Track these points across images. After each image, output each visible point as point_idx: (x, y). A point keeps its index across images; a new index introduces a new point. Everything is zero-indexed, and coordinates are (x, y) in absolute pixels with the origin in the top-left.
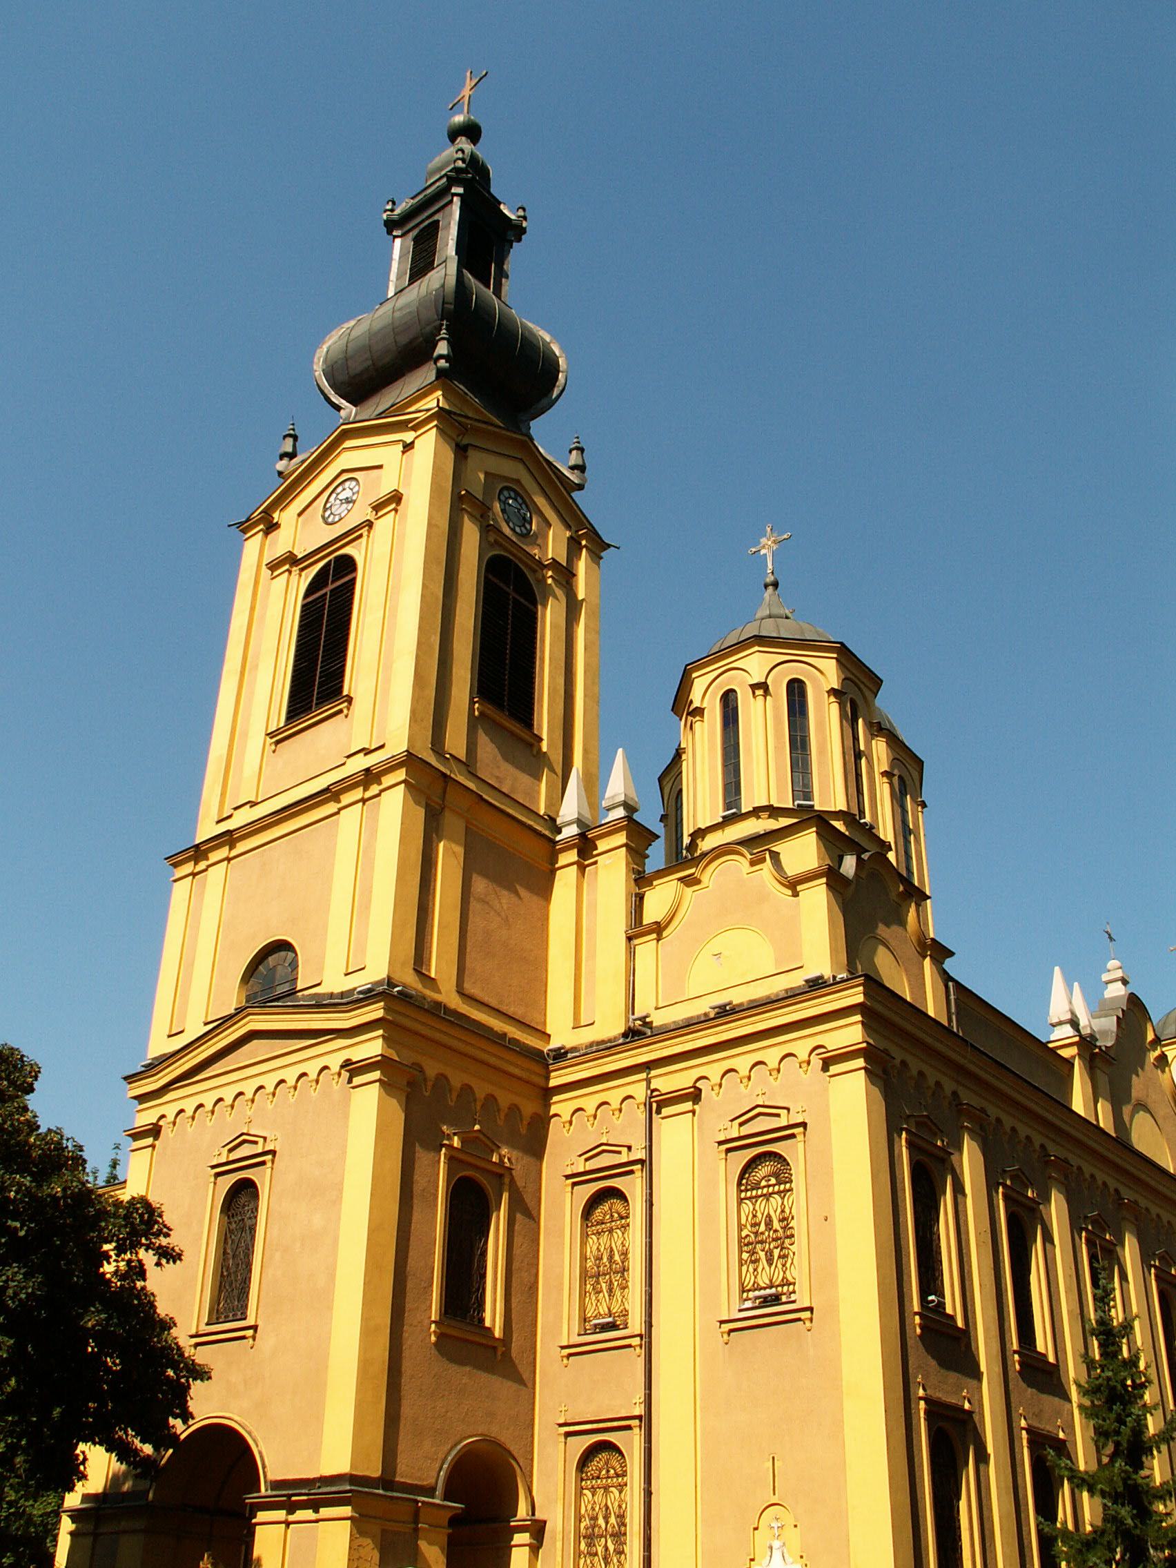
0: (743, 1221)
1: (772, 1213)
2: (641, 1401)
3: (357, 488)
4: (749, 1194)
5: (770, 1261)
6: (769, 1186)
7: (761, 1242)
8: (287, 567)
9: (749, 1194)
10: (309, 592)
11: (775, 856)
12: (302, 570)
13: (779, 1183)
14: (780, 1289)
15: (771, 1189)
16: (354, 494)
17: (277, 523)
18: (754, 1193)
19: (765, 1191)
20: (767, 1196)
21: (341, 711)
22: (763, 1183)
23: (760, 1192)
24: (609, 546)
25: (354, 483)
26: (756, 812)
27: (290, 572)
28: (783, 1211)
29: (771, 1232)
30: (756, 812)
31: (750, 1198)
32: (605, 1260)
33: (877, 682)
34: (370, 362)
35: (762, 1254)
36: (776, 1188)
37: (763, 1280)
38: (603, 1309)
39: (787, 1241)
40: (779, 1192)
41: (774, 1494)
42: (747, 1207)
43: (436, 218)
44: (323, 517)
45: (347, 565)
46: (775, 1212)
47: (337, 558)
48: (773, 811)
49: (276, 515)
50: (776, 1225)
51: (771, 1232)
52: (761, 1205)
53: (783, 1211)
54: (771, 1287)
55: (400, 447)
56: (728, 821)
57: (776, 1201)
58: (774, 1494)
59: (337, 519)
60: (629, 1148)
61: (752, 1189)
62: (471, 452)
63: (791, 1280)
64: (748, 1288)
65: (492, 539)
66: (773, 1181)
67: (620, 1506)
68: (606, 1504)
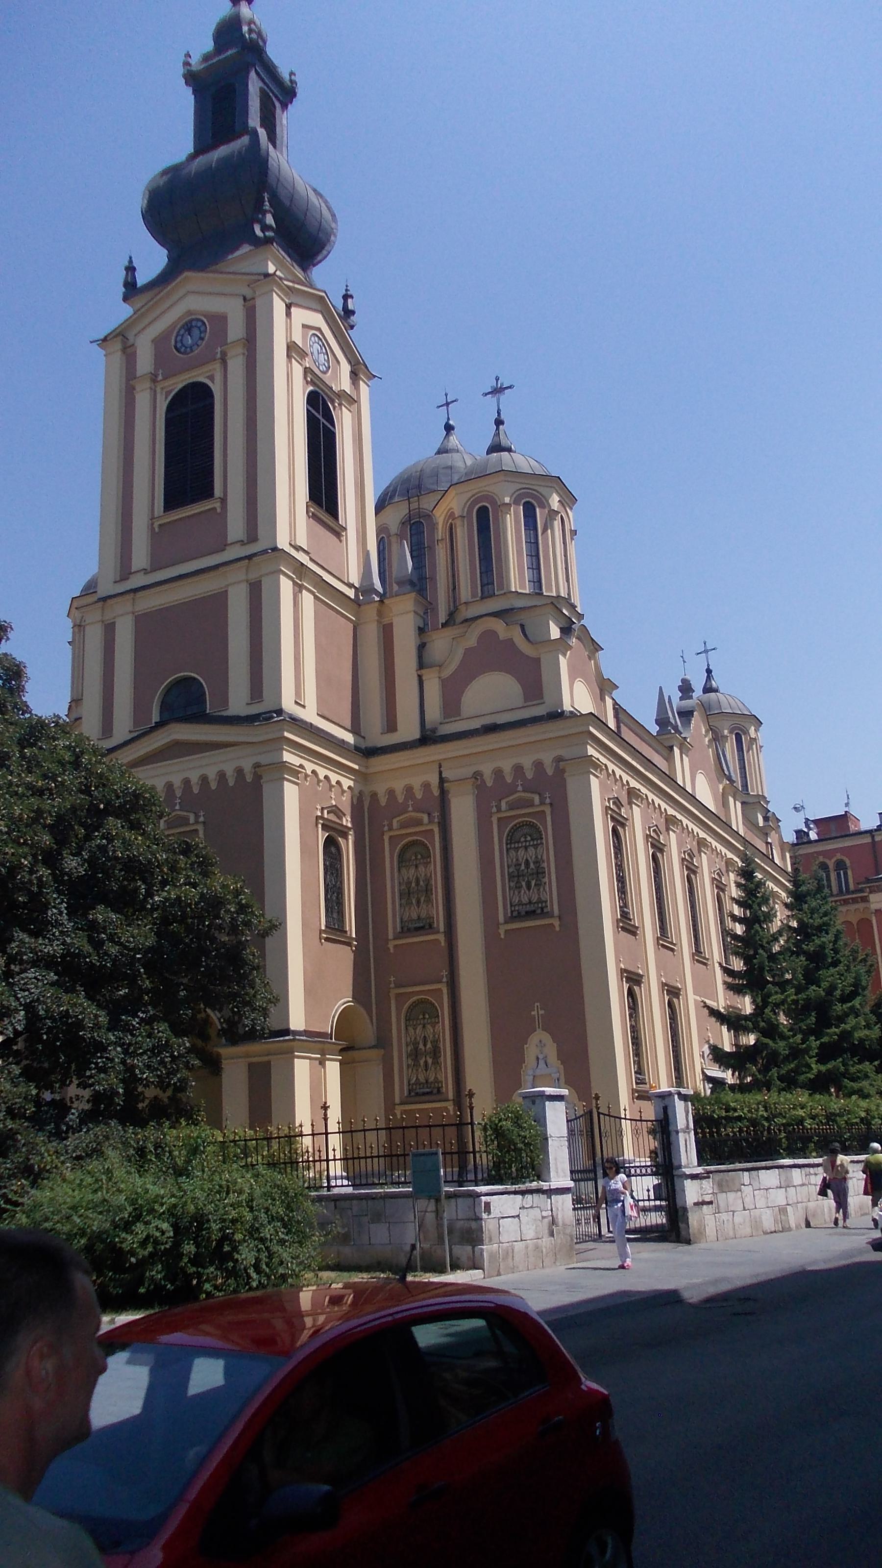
1: (529, 859)
5: (529, 887)
6: (526, 841)
7: (523, 876)
10: (170, 409)
13: (532, 840)
16: (201, 333)
17: (133, 345)
20: (526, 848)
21: (214, 509)
24: (375, 376)
28: (536, 857)
36: (532, 843)
37: (525, 900)
40: (533, 845)
42: (513, 853)
44: (176, 347)
46: (531, 858)
49: (131, 336)
50: (532, 866)
53: (536, 857)
57: (531, 850)
60: (429, 814)
61: (515, 843)
63: (543, 899)
66: (529, 838)
67: (434, 1036)
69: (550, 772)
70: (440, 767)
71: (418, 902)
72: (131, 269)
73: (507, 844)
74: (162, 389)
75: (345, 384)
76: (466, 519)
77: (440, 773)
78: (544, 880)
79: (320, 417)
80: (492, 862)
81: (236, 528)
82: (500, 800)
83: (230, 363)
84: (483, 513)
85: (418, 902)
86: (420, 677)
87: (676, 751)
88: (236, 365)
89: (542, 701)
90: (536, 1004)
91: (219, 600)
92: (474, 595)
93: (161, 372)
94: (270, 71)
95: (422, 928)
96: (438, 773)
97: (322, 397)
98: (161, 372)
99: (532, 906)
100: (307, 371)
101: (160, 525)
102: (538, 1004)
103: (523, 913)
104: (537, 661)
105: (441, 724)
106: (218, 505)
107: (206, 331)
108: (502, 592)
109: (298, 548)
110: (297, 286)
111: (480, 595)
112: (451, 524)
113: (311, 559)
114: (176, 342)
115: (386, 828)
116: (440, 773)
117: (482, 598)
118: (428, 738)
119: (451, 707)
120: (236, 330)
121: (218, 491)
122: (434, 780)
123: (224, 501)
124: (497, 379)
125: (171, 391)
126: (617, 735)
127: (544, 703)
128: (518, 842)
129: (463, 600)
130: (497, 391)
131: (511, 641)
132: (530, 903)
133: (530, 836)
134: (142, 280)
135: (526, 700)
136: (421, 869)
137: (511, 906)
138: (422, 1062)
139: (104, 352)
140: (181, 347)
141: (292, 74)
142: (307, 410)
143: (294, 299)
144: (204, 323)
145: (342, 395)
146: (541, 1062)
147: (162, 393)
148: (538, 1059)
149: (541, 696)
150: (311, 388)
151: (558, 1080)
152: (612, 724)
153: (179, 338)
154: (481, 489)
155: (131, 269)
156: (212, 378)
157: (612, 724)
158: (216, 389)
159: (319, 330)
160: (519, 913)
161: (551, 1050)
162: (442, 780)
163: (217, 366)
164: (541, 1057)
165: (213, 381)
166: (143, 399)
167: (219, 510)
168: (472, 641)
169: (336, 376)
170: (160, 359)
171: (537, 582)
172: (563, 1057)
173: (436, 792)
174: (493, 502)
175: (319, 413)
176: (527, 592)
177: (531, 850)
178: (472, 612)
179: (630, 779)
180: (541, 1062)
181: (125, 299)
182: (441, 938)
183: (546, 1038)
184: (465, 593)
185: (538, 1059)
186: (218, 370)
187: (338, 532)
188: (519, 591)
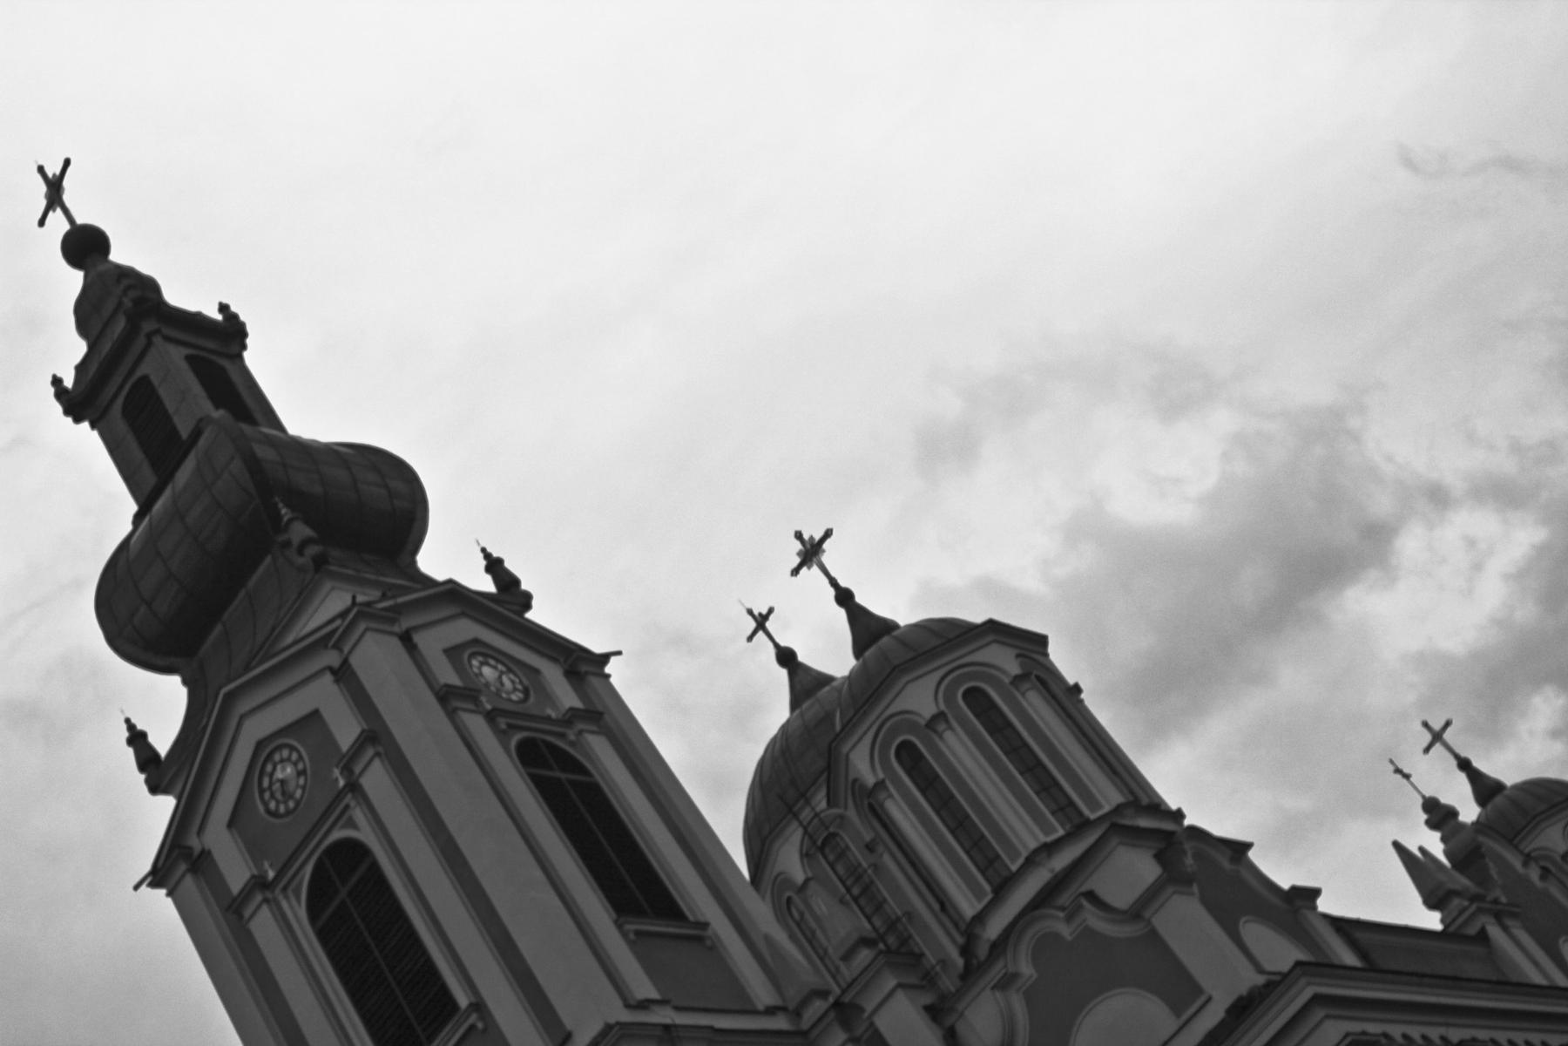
3: (294, 756)
8: (259, 897)
10: (314, 912)
11: (1091, 896)
12: (285, 889)
16: (295, 764)
21: (472, 1027)
25: (285, 753)
26: (1031, 861)
27: (266, 900)
30: (1031, 861)
33: (1041, 641)
43: (139, 373)
44: (268, 812)
45: (353, 852)
48: (1049, 849)
49: (194, 842)
55: (328, 678)
56: (1003, 886)
62: (418, 638)
65: (503, 726)
72: (137, 738)
75: (568, 698)
76: (888, 783)
79: (563, 776)
83: (367, 782)
84: (909, 756)
87: (1494, 931)
88: (377, 779)
89: (1203, 999)
92: (978, 893)
93: (266, 865)
94: (192, 322)
97: (544, 741)
98: (266, 865)
100: (491, 717)
106: (473, 1018)
107: (301, 757)
108: (1020, 861)
109: (644, 1005)
110: (400, 600)
111: (987, 888)
113: (678, 1009)
114: (266, 804)
120: (346, 730)
123: (478, 1006)
124: (799, 536)
125: (300, 884)
126: (1372, 969)
127: (1209, 999)
130: (811, 552)
131: (1088, 933)
134: (162, 742)
135: (1178, 1014)
139: (163, 892)
140: (277, 806)
141: (223, 308)
142: (530, 775)
143: (406, 623)
144: (292, 748)
145: (572, 716)
147: (287, 898)
149: (1197, 990)
150: (516, 738)
152: (1349, 958)
153: (267, 795)
154: (880, 720)
155: (137, 738)
156: (352, 824)
157: (1349, 958)
158: (365, 834)
159: (476, 641)
163: (348, 798)
166: (263, 925)
167: (480, 1025)
169: (547, 697)
170: (255, 849)
171: (1064, 808)
174: (912, 727)
175: (551, 768)
176: (1061, 832)
178: (994, 928)
179: (1442, 1031)
181: (154, 788)
186: (353, 804)
187: (699, 935)
188: (1049, 839)
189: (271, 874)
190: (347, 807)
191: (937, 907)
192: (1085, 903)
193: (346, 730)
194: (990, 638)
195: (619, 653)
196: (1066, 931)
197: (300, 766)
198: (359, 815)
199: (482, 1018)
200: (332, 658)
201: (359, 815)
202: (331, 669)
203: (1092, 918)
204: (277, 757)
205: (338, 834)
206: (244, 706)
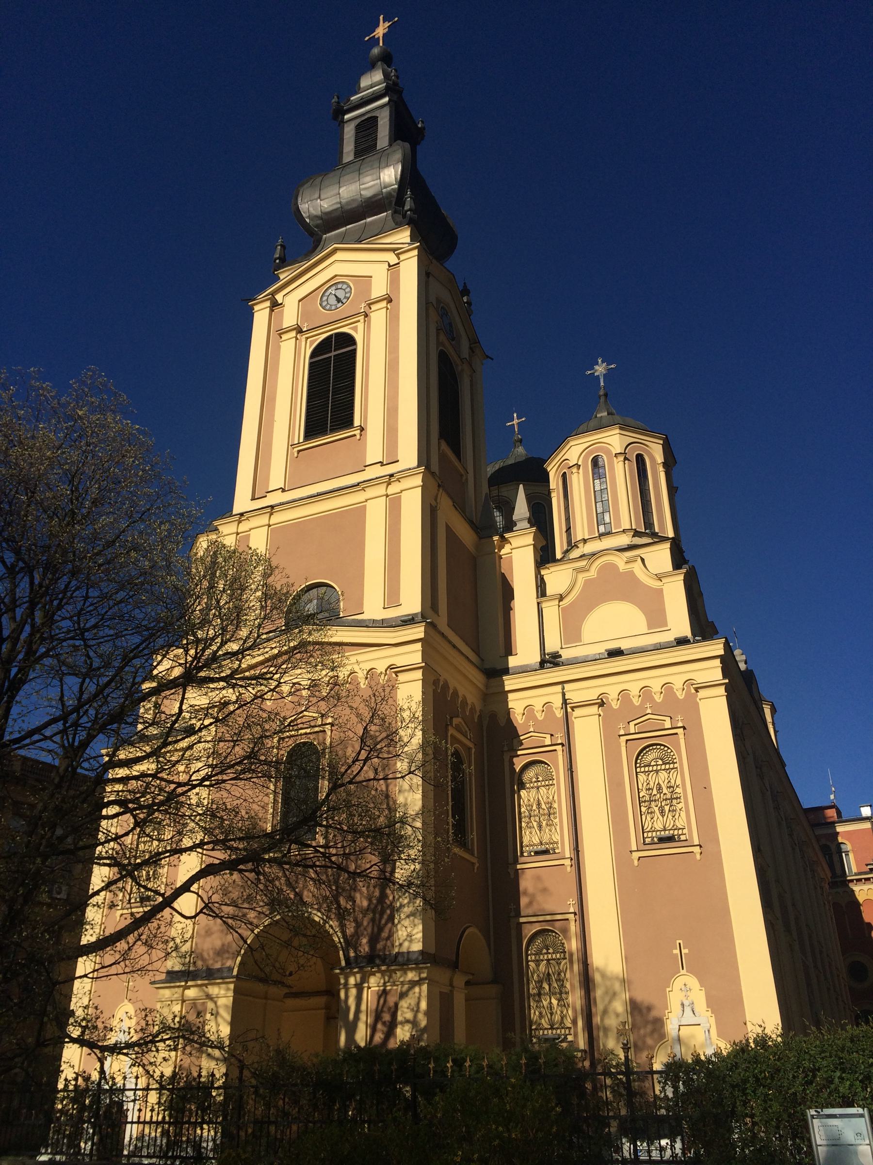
0: (640, 787)
2: (574, 902)
4: (643, 769)
5: (662, 812)
6: (657, 765)
9: (643, 769)
10: (313, 355)
11: (643, 560)
14: (671, 832)
15: (659, 767)
16: (346, 293)
18: (647, 769)
19: (655, 768)
20: (657, 771)
21: (355, 435)
22: (653, 763)
23: (651, 768)
24: (488, 357)
25: (344, 286)
29: (662, 795)
31: (644, 772)
32: (534, 807)
34: (339, 206)
35: (656, 809)
36: (663, 767)
37: (659, 826)
38: (536, 840)
39: (674, 801)
41: (683, 969)
45: (347, 340)
47: (336, 334)
51: (662, 795)
52: (652, 778)
54: (665, 830)
57: (663, 775)
58: (683, 969)
59: (333, 308)
61: (645, 766)
64: (647, 830)
66: (660, 762)
68: (548, 972)
69: (681, 695)
70: (563, 688)
71: (540, 827)
73: (636, 768)
74: (307, 338)
77: (564, 694)
78: (680, 806)
80: (621, 784)
81: (374, 450)
82: (629, 723)
83: (373, 316)
85: (540, 827)
86: (538, 603)
88: (379, 316)
90: (678, 942)
91: (359, 513)
95: (546, 852)
96: (560, 695)
99: (667, 832)
101: (299, 451)
102: (681, 941)
103: (656, 840)
104: (660, 592)
105: (562, 648)
112: (564, 474)
115: (506, 748)
116: (564, 694)
117: (601, 535)
118: (550, 661)
119: (572, 633)
120: (379, 289)
121: (357, 422)
122: (558, 701)
128: (649, 766)
129: (579, 537)
131: (631, 573)
132: (665, 830)
133: (662, 760)
136: (543, 790)
137: (643, 833)
138: (545, 1003)
144: (349, 286)
146: (688, 1010)
148: (683, 1005)
150: (441, 348)
151: (709, 1031)
156: (355, 329)
158: (359, 338)
160: (653, 839)
161: (699, 996)
162: (565, 702)
164: (686, 1003)
165: (356, 331)
168: (593, 573)
171: (649, 524)
172: (712, 1003)
173: (559, 714)
174: (609, 452)
177: (663, 775)
180: (688, 1010)
182: (567, 862)
183: (692, 981)
184: (581, 531)
185: (683, 1005)
189: (305, 329)
190: (359, 321)
191: (564, 529)
192: (639, 560)
193: (379, 289)
194: (661, 442)
195: (492, 359)
196: (622, 566)
197: (348, 295)
198: (360, 326)
199: (361, 435)
200: (392, 258)
201: (360, 326)
202: (389, 264)
203: (637, 567)
204: (339, 286)
205: (345, 330)
206: (339, 256)
